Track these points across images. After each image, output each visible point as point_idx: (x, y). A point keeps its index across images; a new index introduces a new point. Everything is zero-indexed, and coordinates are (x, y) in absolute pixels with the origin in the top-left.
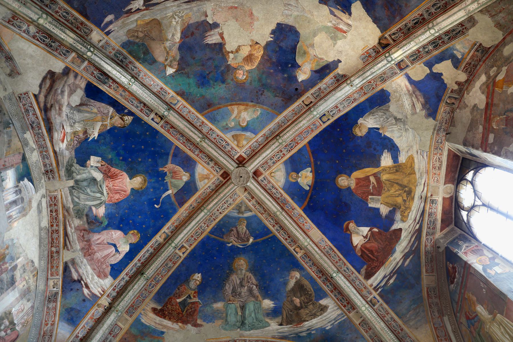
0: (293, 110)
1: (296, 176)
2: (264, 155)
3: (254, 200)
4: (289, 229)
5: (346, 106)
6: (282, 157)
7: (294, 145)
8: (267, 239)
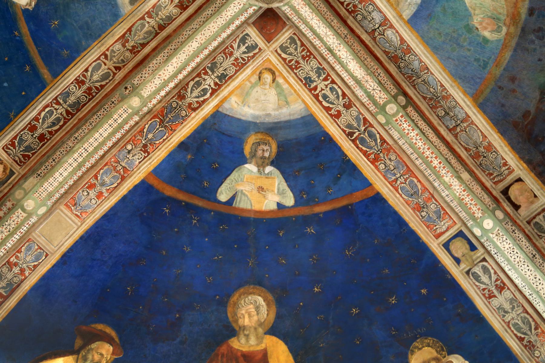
0: (490, 147)
1: (263, 158)
2: (344, 53)
3: (176, 11)
4: (79, 141)
5: (508, 318)
6: (328, 109)
7: (371, 148)
8: (29, 61)
